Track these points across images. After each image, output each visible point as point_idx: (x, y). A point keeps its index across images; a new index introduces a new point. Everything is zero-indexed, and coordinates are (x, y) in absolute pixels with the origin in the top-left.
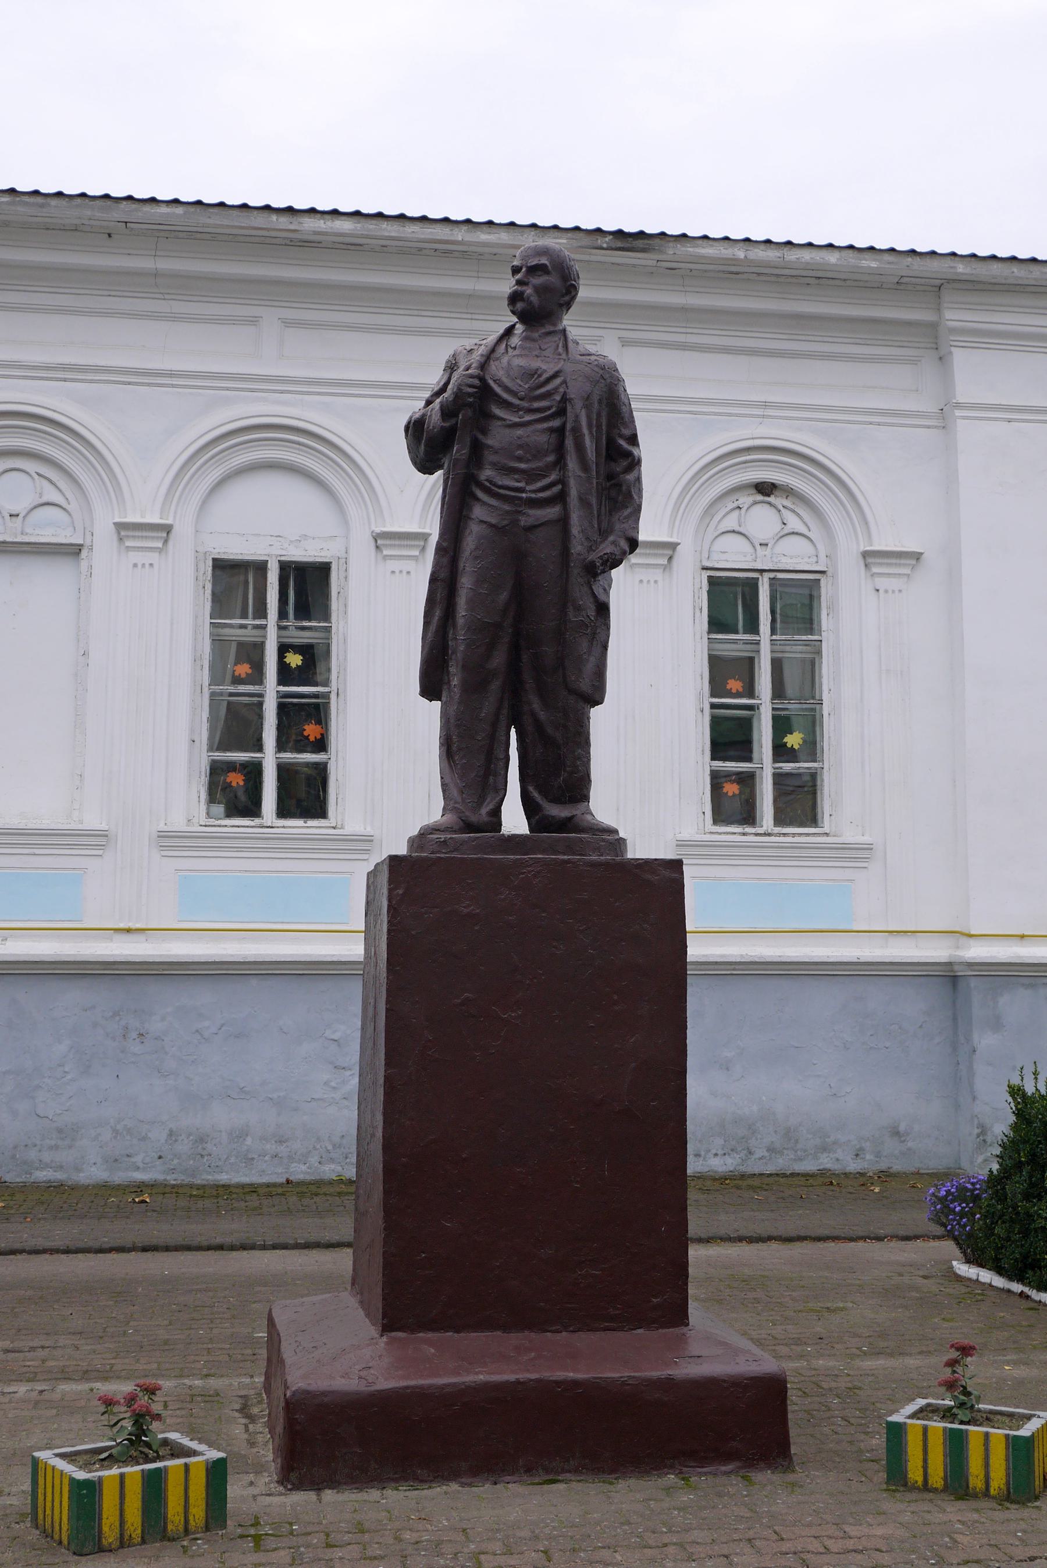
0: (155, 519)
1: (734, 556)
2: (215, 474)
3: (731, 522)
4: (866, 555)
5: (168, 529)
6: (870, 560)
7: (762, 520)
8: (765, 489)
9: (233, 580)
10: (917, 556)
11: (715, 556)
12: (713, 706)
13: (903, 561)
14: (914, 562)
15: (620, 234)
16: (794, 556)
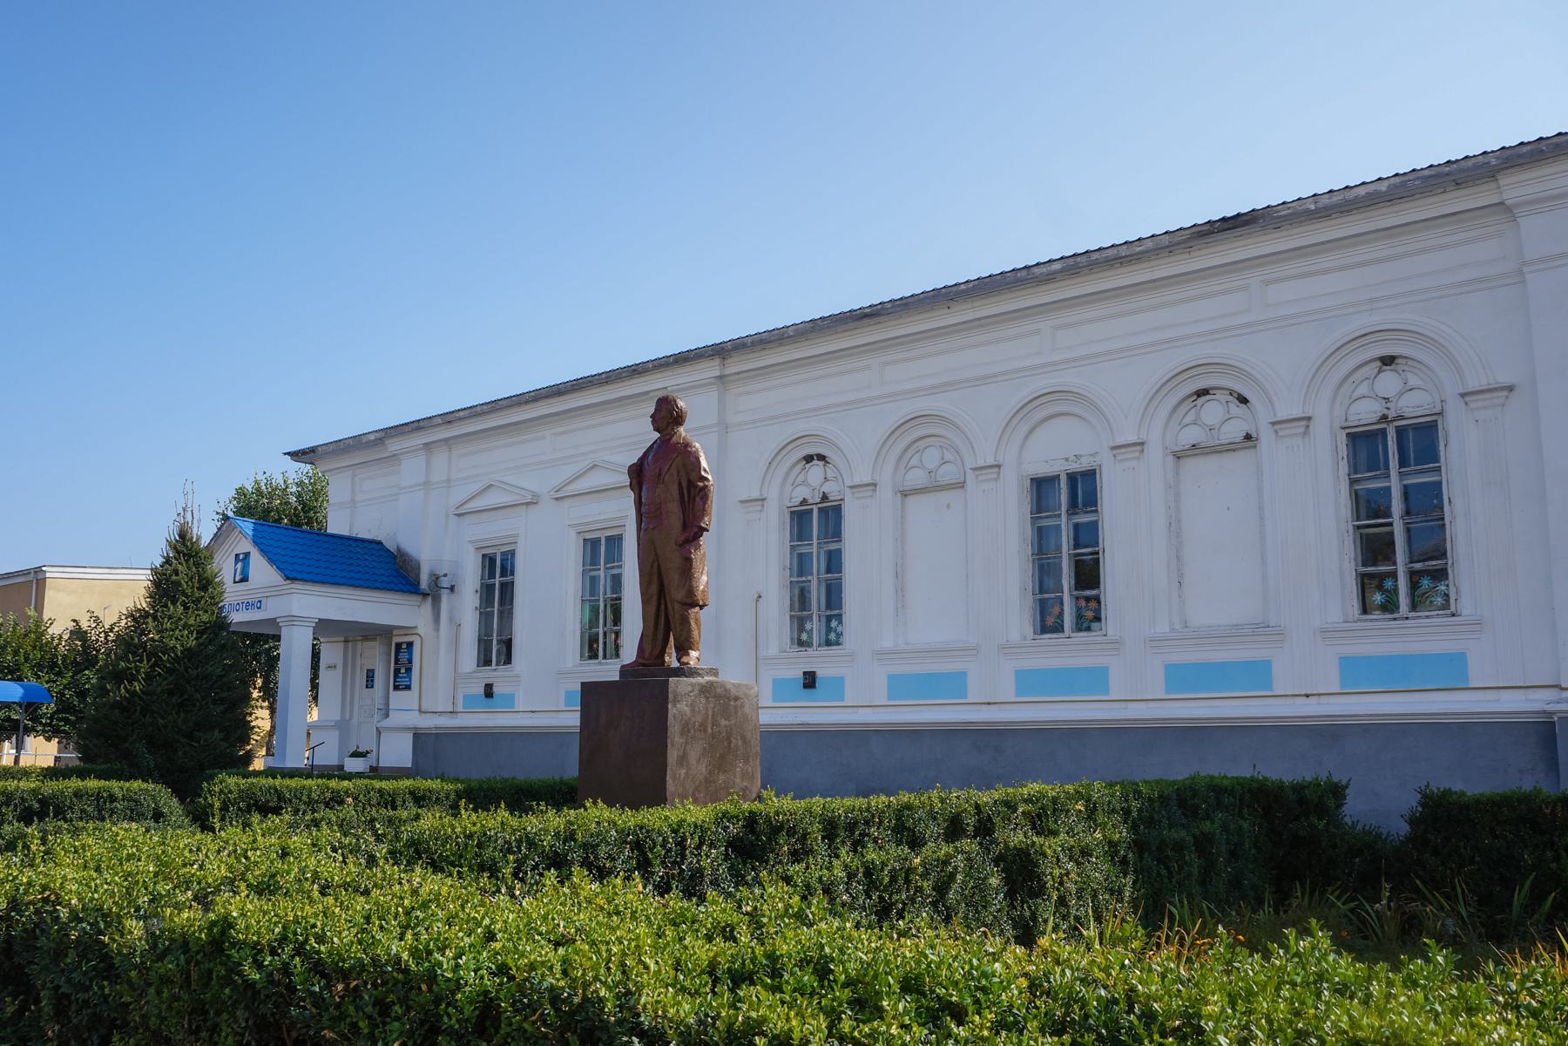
0: (990, 461)
1: (1366, 413)
2: (1025, 429)
3: (1363, 389)
4: (1463, 395)
5: (999, 466)
6: (1467, 399)
7: (1389, 382)
8: (1388, 361)
9: (1041, 486)
10: (1511, 389)
11: (1351, 418)
12: (1359, 527)
13: (1495, 394)
14: (1505, 393)
15: (1224, 219)
16: (1414, 405)
